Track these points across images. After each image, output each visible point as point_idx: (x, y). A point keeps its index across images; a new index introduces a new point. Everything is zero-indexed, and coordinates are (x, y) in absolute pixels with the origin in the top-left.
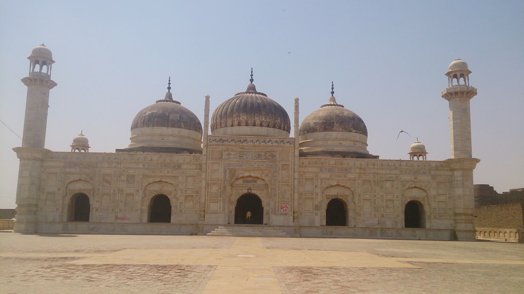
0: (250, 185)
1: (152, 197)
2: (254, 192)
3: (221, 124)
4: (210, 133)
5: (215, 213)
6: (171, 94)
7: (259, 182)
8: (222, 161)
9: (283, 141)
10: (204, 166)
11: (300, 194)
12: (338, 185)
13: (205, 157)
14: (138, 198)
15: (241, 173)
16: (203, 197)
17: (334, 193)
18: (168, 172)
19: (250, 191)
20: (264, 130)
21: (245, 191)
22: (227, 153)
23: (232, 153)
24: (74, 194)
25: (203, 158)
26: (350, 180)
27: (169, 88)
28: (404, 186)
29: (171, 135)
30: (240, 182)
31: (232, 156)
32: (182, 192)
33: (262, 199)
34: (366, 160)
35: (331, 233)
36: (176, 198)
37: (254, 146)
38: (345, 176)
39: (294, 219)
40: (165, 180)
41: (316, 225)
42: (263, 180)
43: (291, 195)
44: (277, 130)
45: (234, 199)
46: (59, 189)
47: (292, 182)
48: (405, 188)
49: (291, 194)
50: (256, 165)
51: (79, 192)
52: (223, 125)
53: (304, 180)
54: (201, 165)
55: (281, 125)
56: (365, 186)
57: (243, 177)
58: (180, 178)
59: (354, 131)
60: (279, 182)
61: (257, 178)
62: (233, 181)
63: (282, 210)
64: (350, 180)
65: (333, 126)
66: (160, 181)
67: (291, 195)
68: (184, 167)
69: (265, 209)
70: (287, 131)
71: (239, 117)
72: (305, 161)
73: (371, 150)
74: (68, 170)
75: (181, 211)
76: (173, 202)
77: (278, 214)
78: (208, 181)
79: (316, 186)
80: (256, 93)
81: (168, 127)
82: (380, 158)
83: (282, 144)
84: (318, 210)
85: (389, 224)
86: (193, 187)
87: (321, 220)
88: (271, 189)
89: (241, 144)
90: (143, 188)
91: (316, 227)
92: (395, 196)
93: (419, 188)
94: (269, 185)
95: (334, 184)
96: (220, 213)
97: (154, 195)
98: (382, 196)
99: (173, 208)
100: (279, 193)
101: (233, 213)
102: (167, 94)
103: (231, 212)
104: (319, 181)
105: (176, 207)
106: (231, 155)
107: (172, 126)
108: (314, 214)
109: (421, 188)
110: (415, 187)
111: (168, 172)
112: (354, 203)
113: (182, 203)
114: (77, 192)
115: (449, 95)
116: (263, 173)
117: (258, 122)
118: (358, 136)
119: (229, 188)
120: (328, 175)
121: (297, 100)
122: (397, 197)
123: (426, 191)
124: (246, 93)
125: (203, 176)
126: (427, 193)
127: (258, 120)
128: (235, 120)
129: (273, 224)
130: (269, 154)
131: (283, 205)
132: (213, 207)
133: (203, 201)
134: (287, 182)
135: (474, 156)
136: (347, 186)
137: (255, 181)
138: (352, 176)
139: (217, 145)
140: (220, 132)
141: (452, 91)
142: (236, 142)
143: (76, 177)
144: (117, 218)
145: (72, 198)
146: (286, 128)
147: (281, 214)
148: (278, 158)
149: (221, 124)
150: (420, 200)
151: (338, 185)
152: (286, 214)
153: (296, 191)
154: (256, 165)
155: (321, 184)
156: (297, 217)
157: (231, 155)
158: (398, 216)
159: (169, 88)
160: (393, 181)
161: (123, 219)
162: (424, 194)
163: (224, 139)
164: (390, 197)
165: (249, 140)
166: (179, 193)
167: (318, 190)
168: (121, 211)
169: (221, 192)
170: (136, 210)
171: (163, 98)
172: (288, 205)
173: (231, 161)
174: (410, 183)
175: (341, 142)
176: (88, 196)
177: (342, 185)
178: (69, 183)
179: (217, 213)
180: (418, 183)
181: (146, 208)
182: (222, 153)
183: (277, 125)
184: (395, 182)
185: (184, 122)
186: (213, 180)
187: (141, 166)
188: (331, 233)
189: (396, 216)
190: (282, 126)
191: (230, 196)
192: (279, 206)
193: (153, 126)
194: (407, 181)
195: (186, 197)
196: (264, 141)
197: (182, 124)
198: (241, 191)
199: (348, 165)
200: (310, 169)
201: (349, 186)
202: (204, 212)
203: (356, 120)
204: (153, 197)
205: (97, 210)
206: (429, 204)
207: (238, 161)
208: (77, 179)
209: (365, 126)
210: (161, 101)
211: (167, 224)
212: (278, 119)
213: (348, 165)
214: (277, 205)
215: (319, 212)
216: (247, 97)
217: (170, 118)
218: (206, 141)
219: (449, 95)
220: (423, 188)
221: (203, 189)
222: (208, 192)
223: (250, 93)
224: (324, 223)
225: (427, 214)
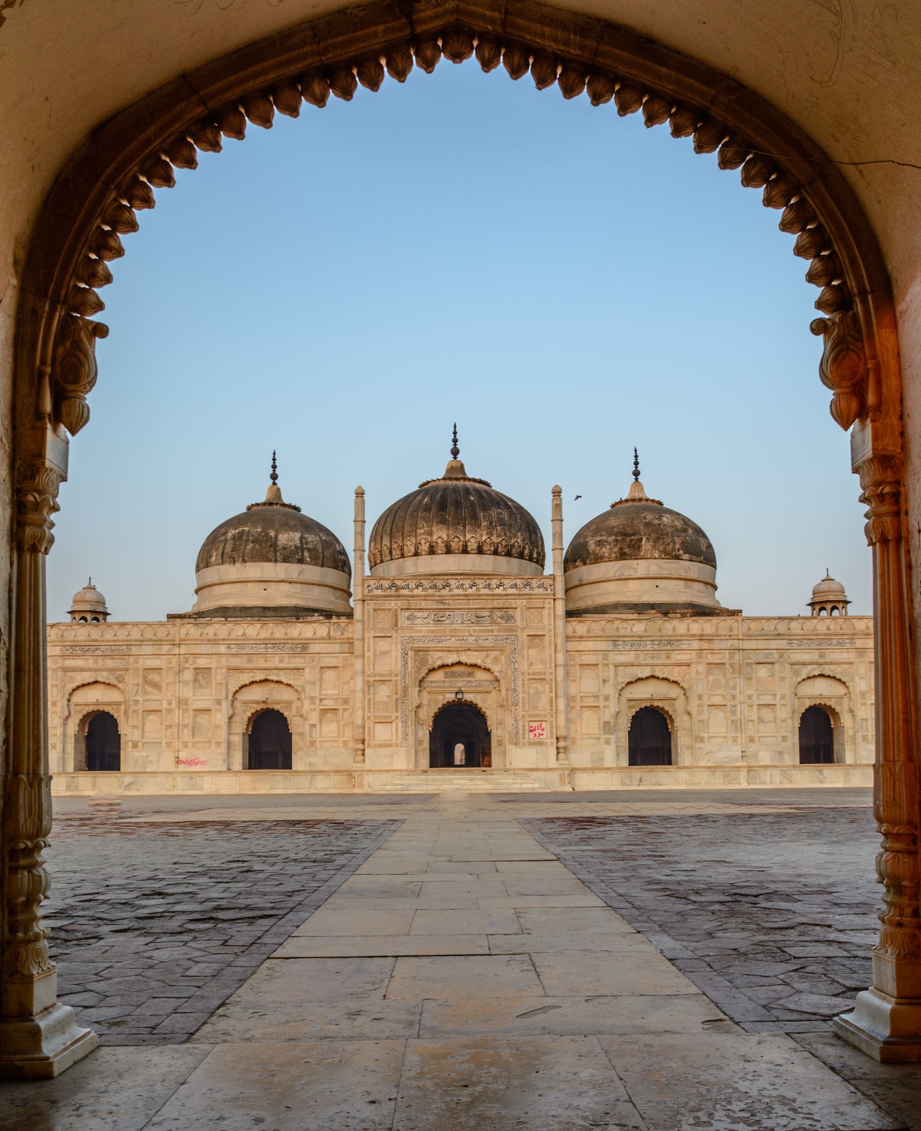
0: (460, 683)
1: (249, 714)
2: (468, 697)
3: (391, 552)
4: (367, 572)
5: (387, 746)
6: (279, 490)
7: (480, 675)
8: (397, 632)
9: (528, 584)
10: (358, 645)
11: (570, 699)
12: (653, 677)
13: (360, 624)
14: (221, 717)
15: (437, 659)
16: (360, 713)
17: (645, 693)
18: (281, 661)
19: (460, 696)
20: (486, 563)
21: (451, 697)
22: (407, 614)
23: (419, 614)
24: (84, 713)
25: (355, 630)
26: (680, 665)
27: (274, 477)
28: (796, 673)
29: (283, 581)
30: (439, 676)
31: (419, 621)
32: (313, 703)
33: (488, 713)
34: (715, 620)
35: (641, 780)
36: (302, 716)
37: (466, 595)
38: (668, 658)
39: (558, 753)
40: (275, 678)
41: (606, 765)
42: (489, 670)
43: (551, 702)
44: (515, 562)
45: (428, 714)
47: (551, 674)
48: (800, 679)
49: (551, 698)
50: (471, 639)
51: (95, 708)
52: (396, 553)
53: (578, 667)
55: (524, 548)
56: (711, 678)
57: (443, 666)
58: (307, 671)
59: (686, 556)
60: (523, 674)
61: (475, 666)
62: (424, 674)
63: (532, 734)
64: (680, 665)
65: (639, 547)
66: (266, 680)
67: (551, 702)
68: (315, 648)
69: (496, 734)
70: (537, 562)
71: (431, 534)
72: (579, 627)
73: (724, 598)
74: (70, 663)
75: (313, 743)
76: (296, 725)
77: (524, 744)
78: (369, 676)
79: (604, 681)
80: (466, 479)
81: (276, 561)
82: (744, 614)
83: (527, 591)
84: (611, 734)
85: (765, 758)
86: (336, 692)
87: (618, 755)
88: (507, 690)
89: (437, 593)
90: (231, 695)
91: (608, 769)
92: (778, 697)
93: (829, 676)
94: (502, 682)
95: (644, 676)
96: (397, 745)
97: (254, 711)
98: (750, 697)
99: (294, 738)
100: (523, 698)
101: (426, 744)
102: (270, 488)
103: (419, 742)
104: (612, 668)
105: (301, 734)
106: (416, 618)
107: (286, 560)
108: (602, 741)
109: (834, 678)
110: (822, 676)
111: (281, 661)
112: (689, 714)
113: (314, 725)
114: (91, 709)
116: (487, 656)
117: (473, 545)
118: (707, 568)
119: (414, 691)
120: (630, 657)
122: (783, 697)
123: (844, 683)
124: (444, 479)
125: (358, 666)
126: (847, 687)
127: (473, 540)
128: (423, 541)
129: (513, 766)
130: (499, 613)
131: (534, 724)
132: (382, 733)
133: (359, 721)
134: (540, 673)
136: (672, 679)
137: (470, 674)
138: (683, 657)
140: (391, 568)
142: (425, 589)
143: (88, 677)
144: (178, 762)
145: (82, 722)
146: (535, 555)
147: (530, 744)
148: (519, 623)
149: (391, 552)
150: (832, 703)
151: (653, 677)
152: (541, 744)
153: (561, 693)
154: (471, 639)
155: (616, 676)
156: (565, 748)
157: (416, 618)
158: (784, 739)
160: (773, 663)
161: (191, 763)
162: (841, 690)
163: (399, 583)
164: (768, 699)
165: (453, 583)
166: (307, 704)
167: (610, 690)
168: (185, 745)
169: (397, 700)
170: (218, 744)
171: (262, 499)
172: (544, 725)
173: (416, 632)
174: (810, 667)
175: (658, 582)
177: (661, 676)
178: (74, 690)
179: (391, 745)
180: (826, 666)
181: (238, 740)
182: (396, 616)
183: (514, 551)
184: (777, 665)
185: (309, 550)
186: (380, 675)
188: (641, 780)
189: (780, 739)
190: (526, 552)
191: (418, 707)
192: (524, 726)
193: (244, 561)
194: (804, 664)
195: (324, 712)
196: (488, 586)
197: (306, 554)
198: (441, 697)
199: (674, 629)
200: (591, 645)
201: (676, 679)
202: (363, 742)
203: (690, 531)
204: (253, 714)
205: (135, 746)
206: (851, 711)
207: (433, 631)
208: (91, 680)
209: (710, 546)
211: (286, 772)
212: (515, 536)
213: (674, 629)
214: (520, 723)
215: (612, 738)
216: (446, 489)
217: (279, 543)
218: (359, 589)
220: (838, 676)
221: (359, 695)
222: (369, 700)
223: (450, 479)
224: (625, 762)
225: (849, 733)
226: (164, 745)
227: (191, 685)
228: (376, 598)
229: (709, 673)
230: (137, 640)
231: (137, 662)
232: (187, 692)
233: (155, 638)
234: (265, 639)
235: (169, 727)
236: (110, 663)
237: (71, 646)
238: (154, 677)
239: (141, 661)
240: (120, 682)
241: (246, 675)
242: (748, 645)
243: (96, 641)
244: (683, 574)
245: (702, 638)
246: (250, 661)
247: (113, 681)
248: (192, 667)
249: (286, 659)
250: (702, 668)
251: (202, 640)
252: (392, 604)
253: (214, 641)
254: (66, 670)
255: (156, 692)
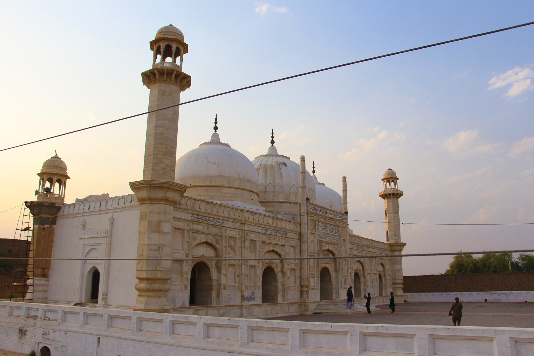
32: (288, 265)
46: (187, 256)
54: (300, 235)
58: (287, 247)
68: (289, 235)
74: (196, 227)
75: (289, 287)
113: (289, 278)
115: (384, 196)
121: (344, 179)
130: (337, 228)
135: (402, 241)
139: (313, 213)
141: (387, 193)
159: (216, 128)
165: (328, 212)
176: (210, 266)
187: (260, 230)
202: (307, 287)
210: (206, 143)
219: (384, 196)
226: (237, 287)
227: (249, 250)
228: (311, 213)
230: (227, 217)
231: (225, 232)
232: (247, 254)
233: (234, 218)
234: (274, 227)
235: (238, 276)
236: (214, 230)
237: (197, 215)
238: (232, 243)
239: (228, 231)
240: (217, 244)
241: (267, 247)
243: (209, 214)
246: (269, 239)
247: (214, 243)
248: (249, 239)
249: (281, 240)
251: (253, 223)
253: (257, 225)
254: (194, 231)
255: (232, 252)
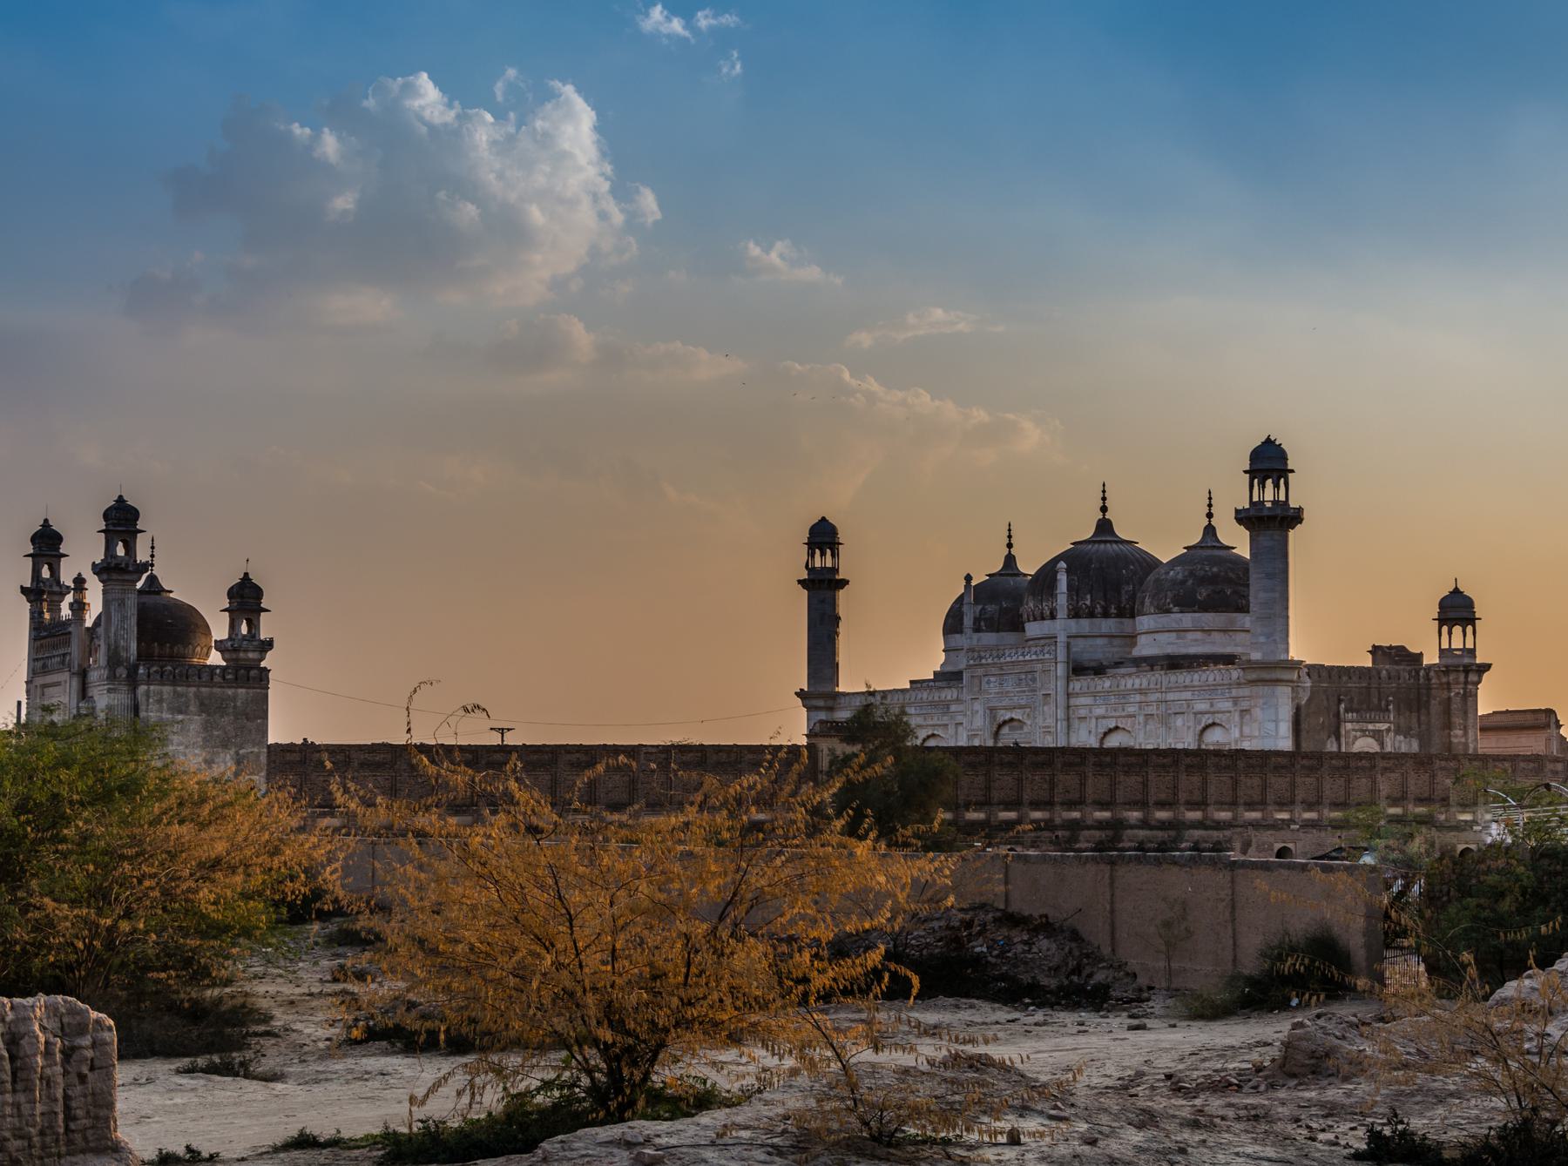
68: (953, 708)
138: (1131, 709)
229: (1146, 723)
242: (1171, 696)
244: (1175, 626)
245: (1141, 691)
250: (1141, 719)
252: (980, 671)
